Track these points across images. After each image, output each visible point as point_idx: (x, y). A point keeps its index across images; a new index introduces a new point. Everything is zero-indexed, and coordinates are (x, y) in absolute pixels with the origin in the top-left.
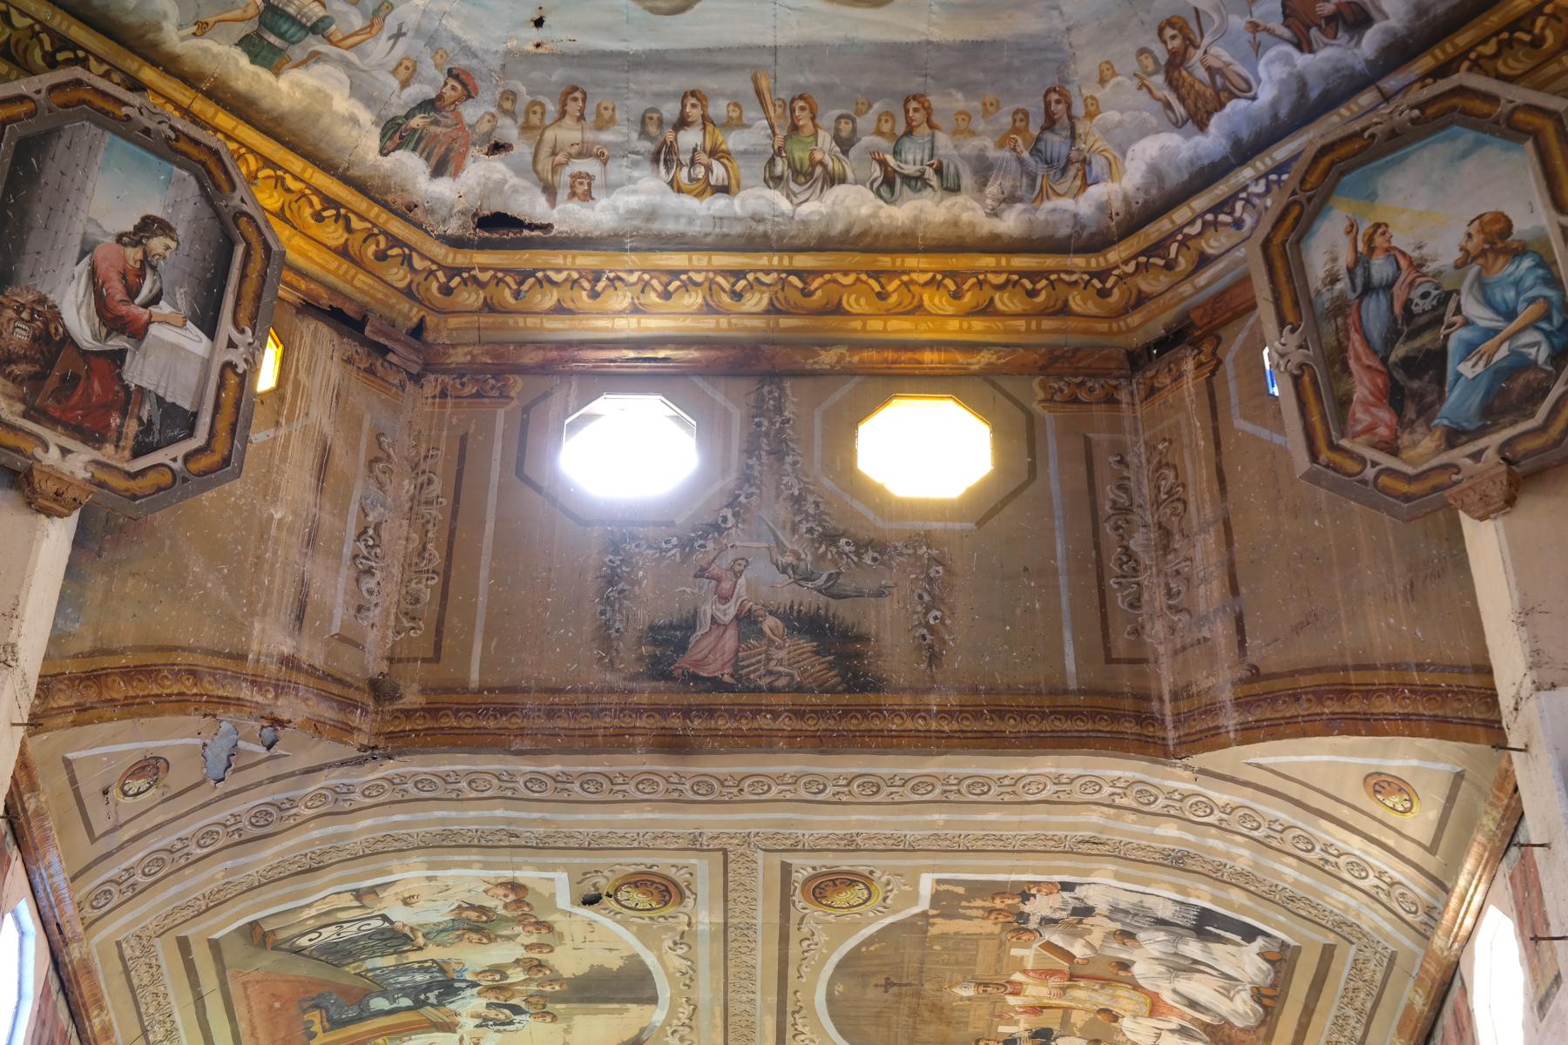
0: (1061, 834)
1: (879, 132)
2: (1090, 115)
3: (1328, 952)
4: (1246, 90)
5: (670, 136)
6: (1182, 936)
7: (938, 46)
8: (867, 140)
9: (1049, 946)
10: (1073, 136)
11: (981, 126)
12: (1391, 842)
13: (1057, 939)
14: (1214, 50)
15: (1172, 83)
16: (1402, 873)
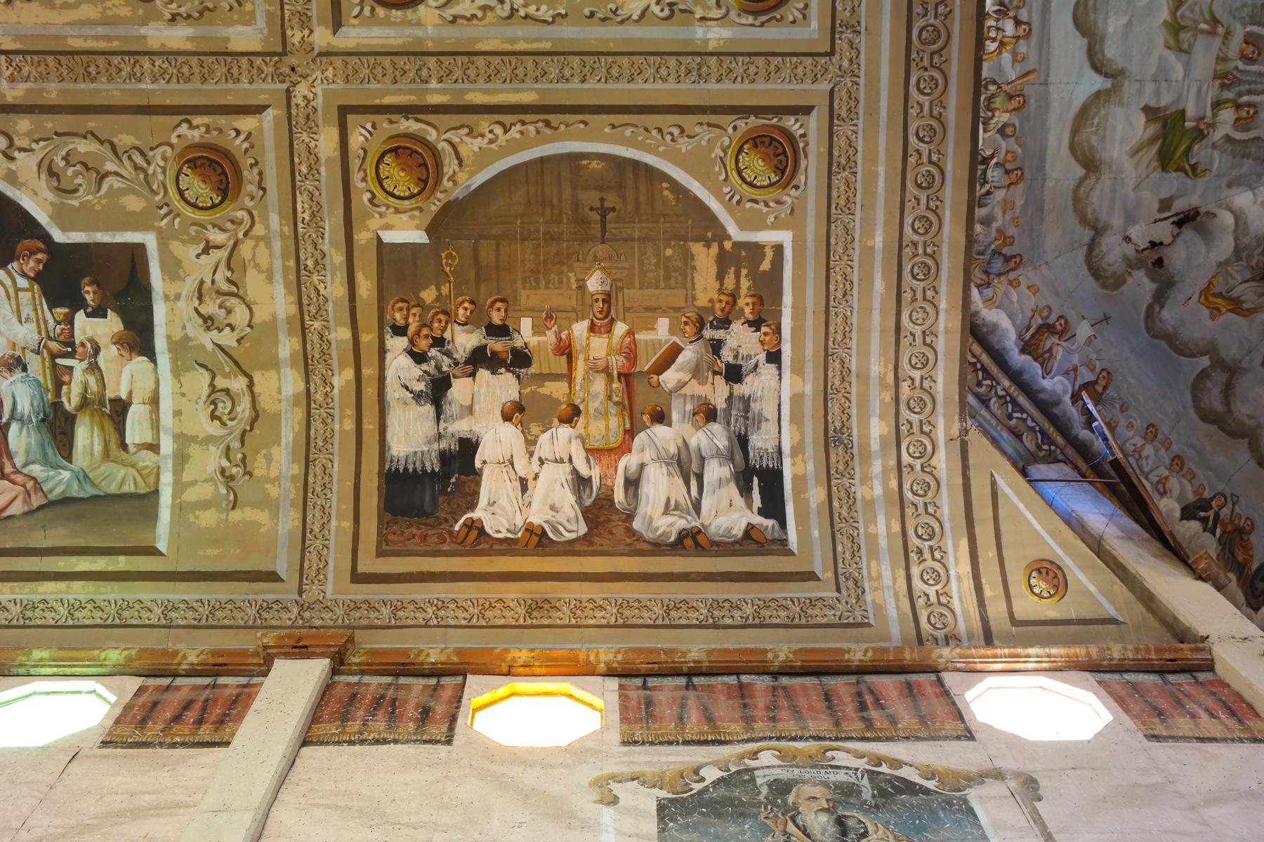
0: (854, 344)
1: (1007, 152)
2: (1010, 283)
3: (810, 576)
4: (1047, 373)
5: (1011, 14)
6: (732, 459)
7: (1043, 186)
8: (1004, 144)
9: (675, 351)
10: (1000, 275)
11: (1008, 217)
12: (988, 592)
13: (688, 354)
14: (1060, 349)
15: (1040, 327)
16: (964, 611)
